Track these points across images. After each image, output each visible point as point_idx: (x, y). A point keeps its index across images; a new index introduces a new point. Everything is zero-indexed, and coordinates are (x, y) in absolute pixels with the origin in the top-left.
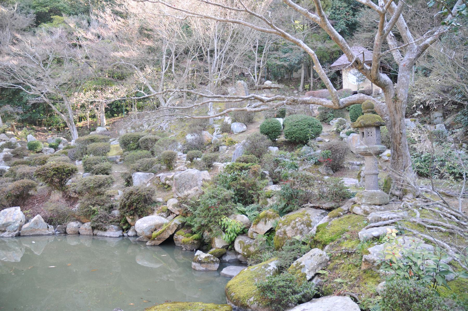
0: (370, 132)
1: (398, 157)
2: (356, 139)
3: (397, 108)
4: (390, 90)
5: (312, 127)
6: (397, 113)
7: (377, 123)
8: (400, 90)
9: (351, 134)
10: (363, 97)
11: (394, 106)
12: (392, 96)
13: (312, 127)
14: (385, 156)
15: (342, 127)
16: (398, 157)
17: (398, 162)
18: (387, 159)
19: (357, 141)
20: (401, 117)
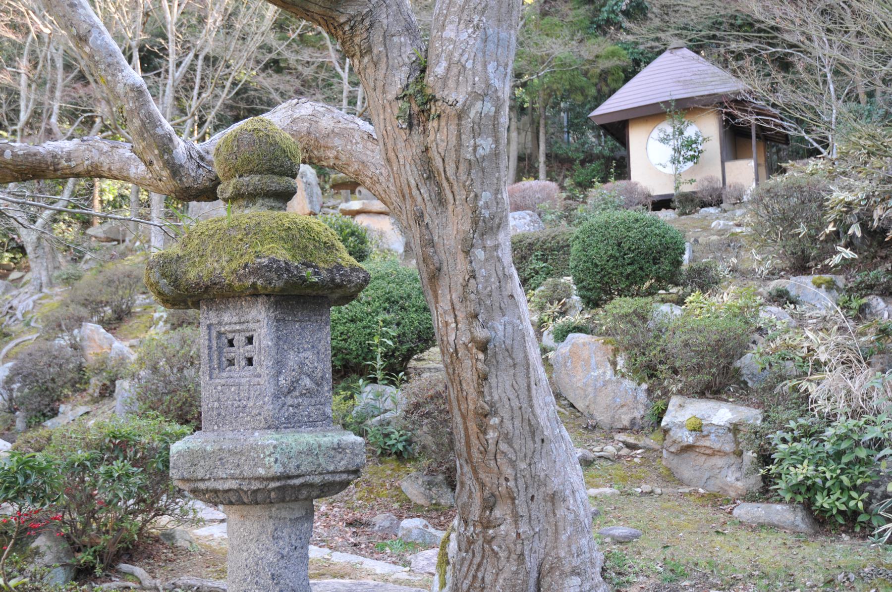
0: (240, 339)
1: (489, 505)
2: (585, 354)
3: (438, 162)
4: (377, 37)
5: (403, 308)
6: (441, 202)
7: (256, 271)
8: (450, 32)
9: (570, 335)
10: (313, 118)
11: (417, 151)
12: (399, 79)
13: (403, 308)
14: (681, 426)
15: (556, 307)
16: (489, 505)
17: (489, 541)
18: (691, 440)
19: (587, 362)
20: (467, 226)
